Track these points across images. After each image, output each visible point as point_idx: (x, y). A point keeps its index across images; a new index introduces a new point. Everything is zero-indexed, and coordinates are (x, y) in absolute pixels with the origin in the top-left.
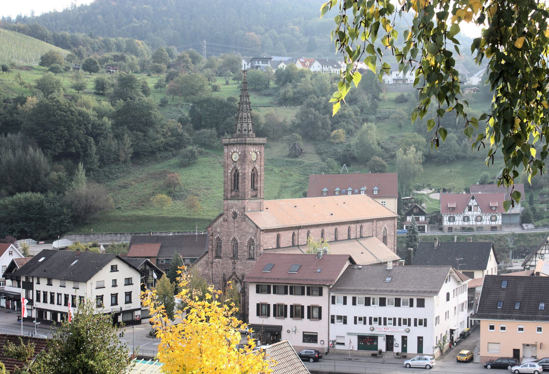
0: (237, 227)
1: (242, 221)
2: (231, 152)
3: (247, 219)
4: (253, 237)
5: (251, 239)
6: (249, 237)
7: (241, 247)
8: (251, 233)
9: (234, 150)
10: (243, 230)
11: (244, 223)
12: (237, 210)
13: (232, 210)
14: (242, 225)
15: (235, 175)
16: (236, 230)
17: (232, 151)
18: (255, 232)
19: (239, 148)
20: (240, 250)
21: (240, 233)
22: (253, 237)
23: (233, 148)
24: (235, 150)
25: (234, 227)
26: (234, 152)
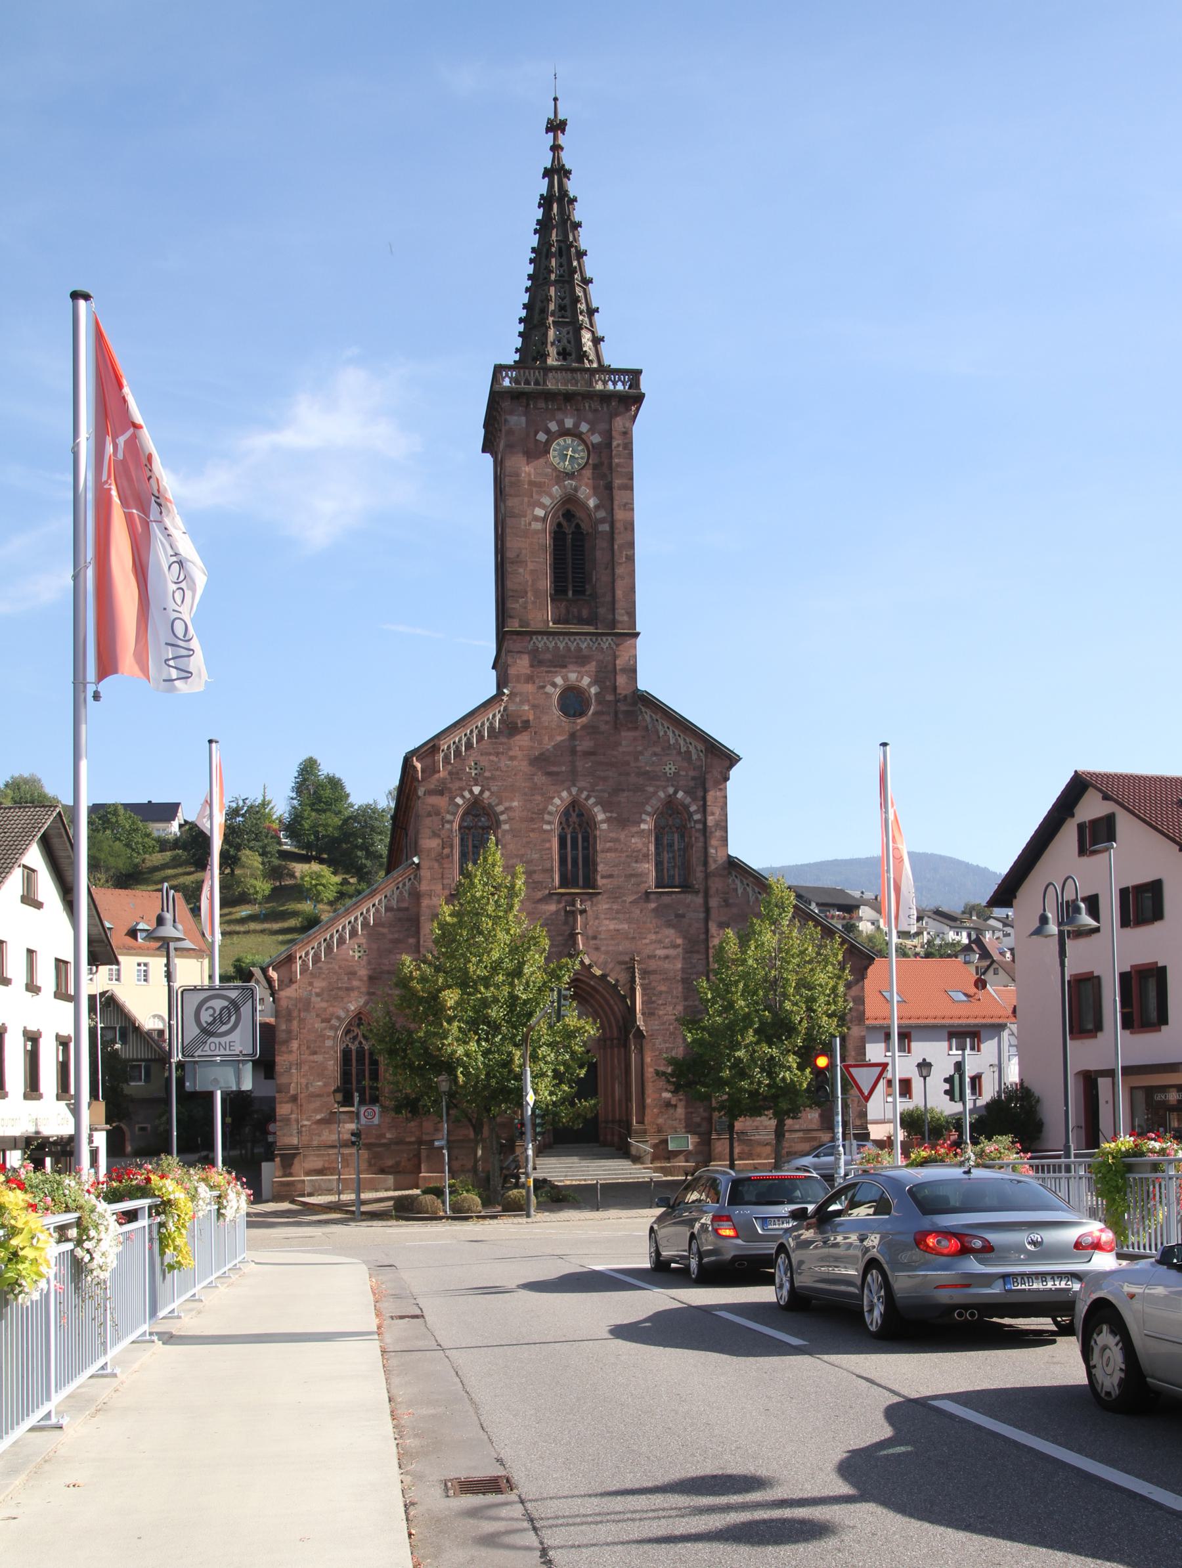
0: (589, 754)
1: (617, 727)
2: (548, 431)
3: (647, 716)
4: (680, 795)
5: (670, 803)
6: (661, 794)
7: (617, 840)
8: (668, 780)
9: (561, 423)
10: (628, 763)
11: (626, 736)
12: (586, 681)
13: (559, 680)
14: (617, 744)
15: (558, 536)
16: (583, 765)
17: (553, 426)
18: (692, 773)
19: (590, 416)
20: (609, 850)
21: (605, 779)
22: (680, 795)
23: (559, 416)
24: (569, 423)
25: (573, 752)
26: (565, 433)
